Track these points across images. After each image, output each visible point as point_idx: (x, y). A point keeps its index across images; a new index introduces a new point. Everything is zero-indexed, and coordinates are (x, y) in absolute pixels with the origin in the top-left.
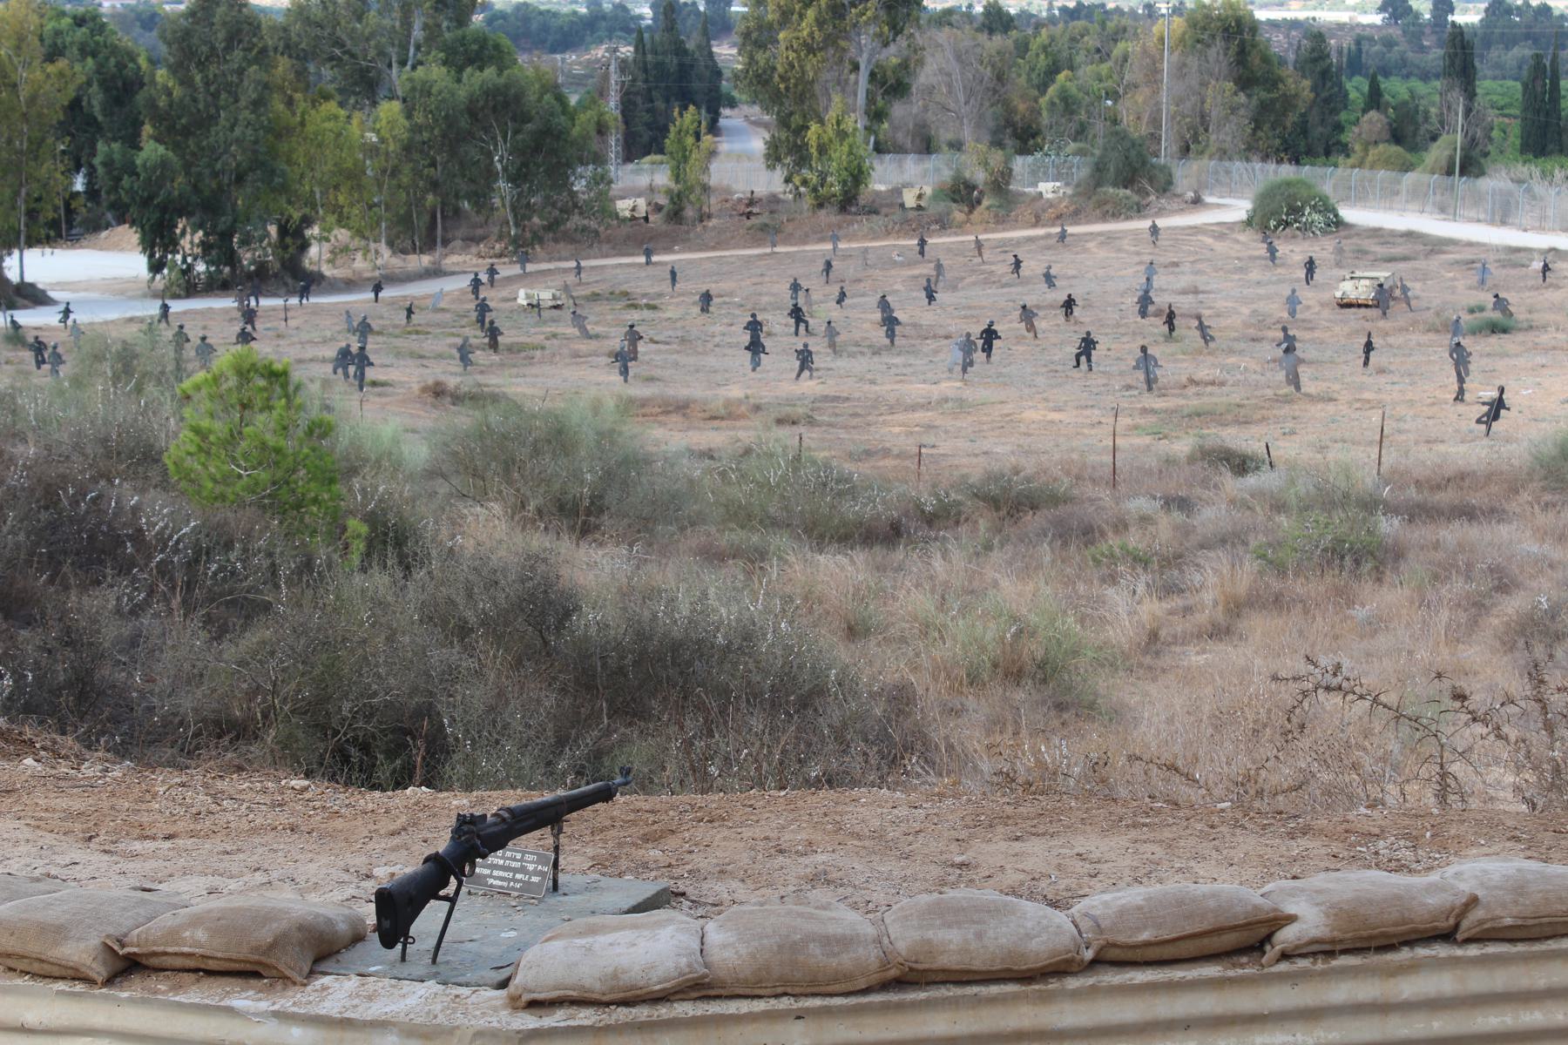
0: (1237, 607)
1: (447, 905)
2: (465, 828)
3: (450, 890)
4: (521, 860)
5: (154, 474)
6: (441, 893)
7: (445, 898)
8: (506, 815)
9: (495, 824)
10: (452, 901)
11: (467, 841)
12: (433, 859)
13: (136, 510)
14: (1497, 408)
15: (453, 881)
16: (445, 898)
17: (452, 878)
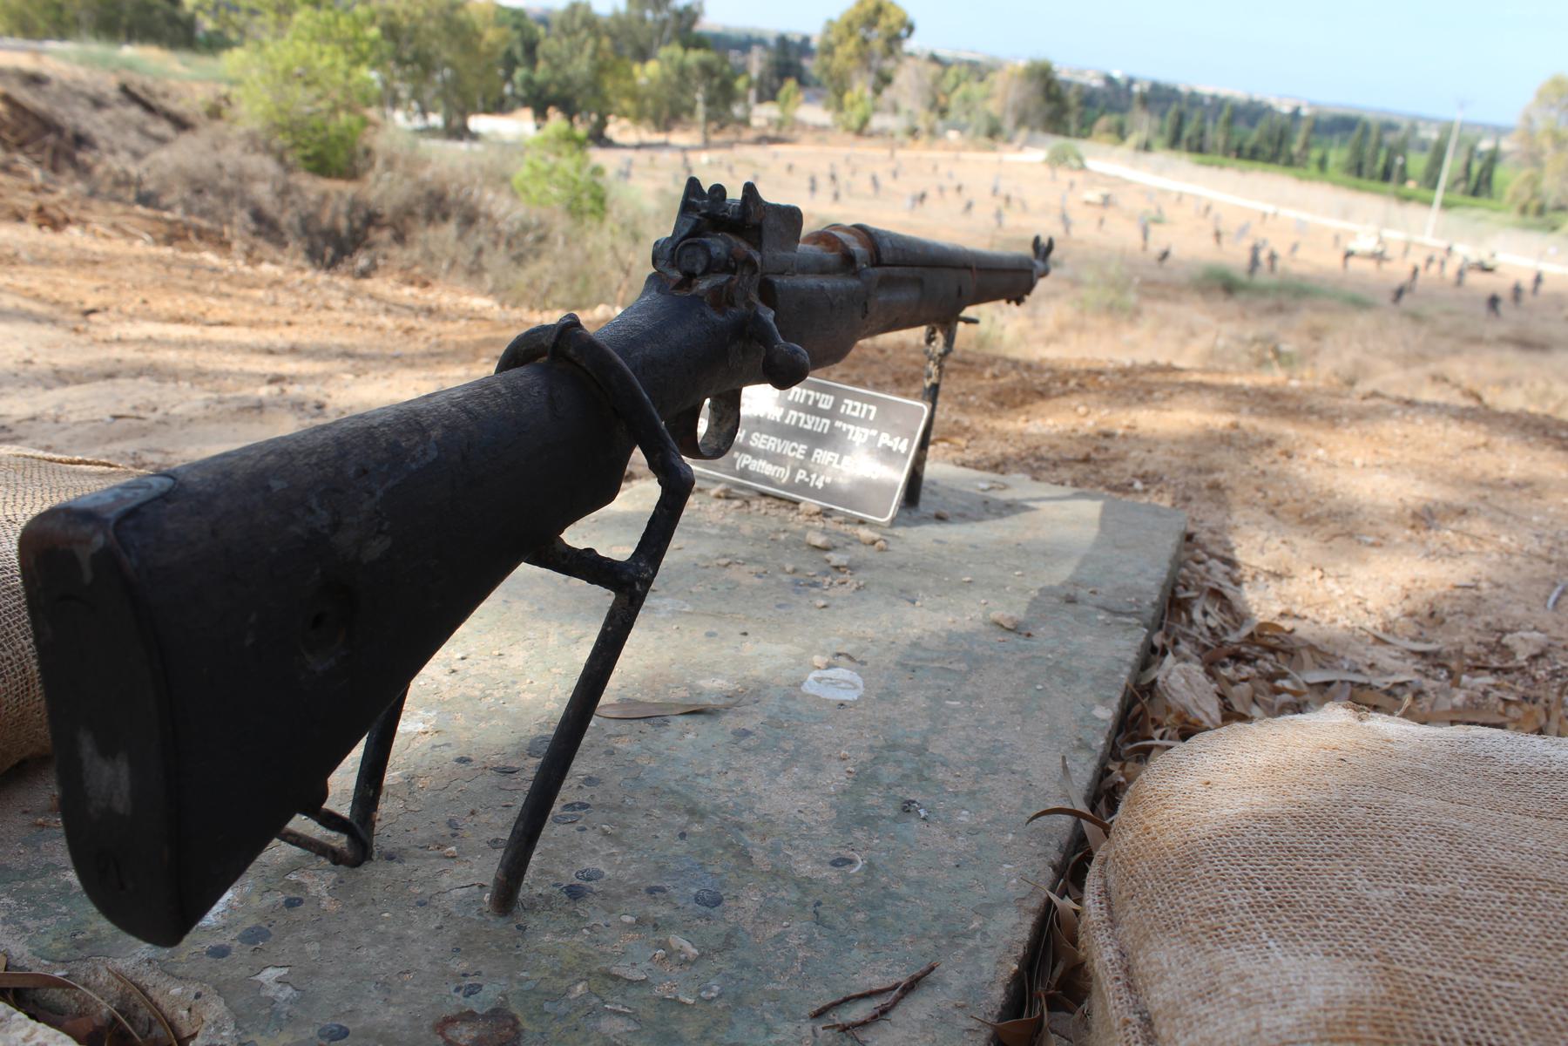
0: (1062, 328)
1: (603, 598)
2: (718, 245)
3: (611, 529)
4: (832, 414)
5: (506, 187)
6: (576, 536)
7: (587, 566)
8: (856, 247)
9: (823, 269)
10: (627, 585)
11: (721, 299)
12: (553, 355)
13: (493, 202)
14: (1165, 255)
15: (639, 495)
16: (587, 566)
17: (638, 457)
